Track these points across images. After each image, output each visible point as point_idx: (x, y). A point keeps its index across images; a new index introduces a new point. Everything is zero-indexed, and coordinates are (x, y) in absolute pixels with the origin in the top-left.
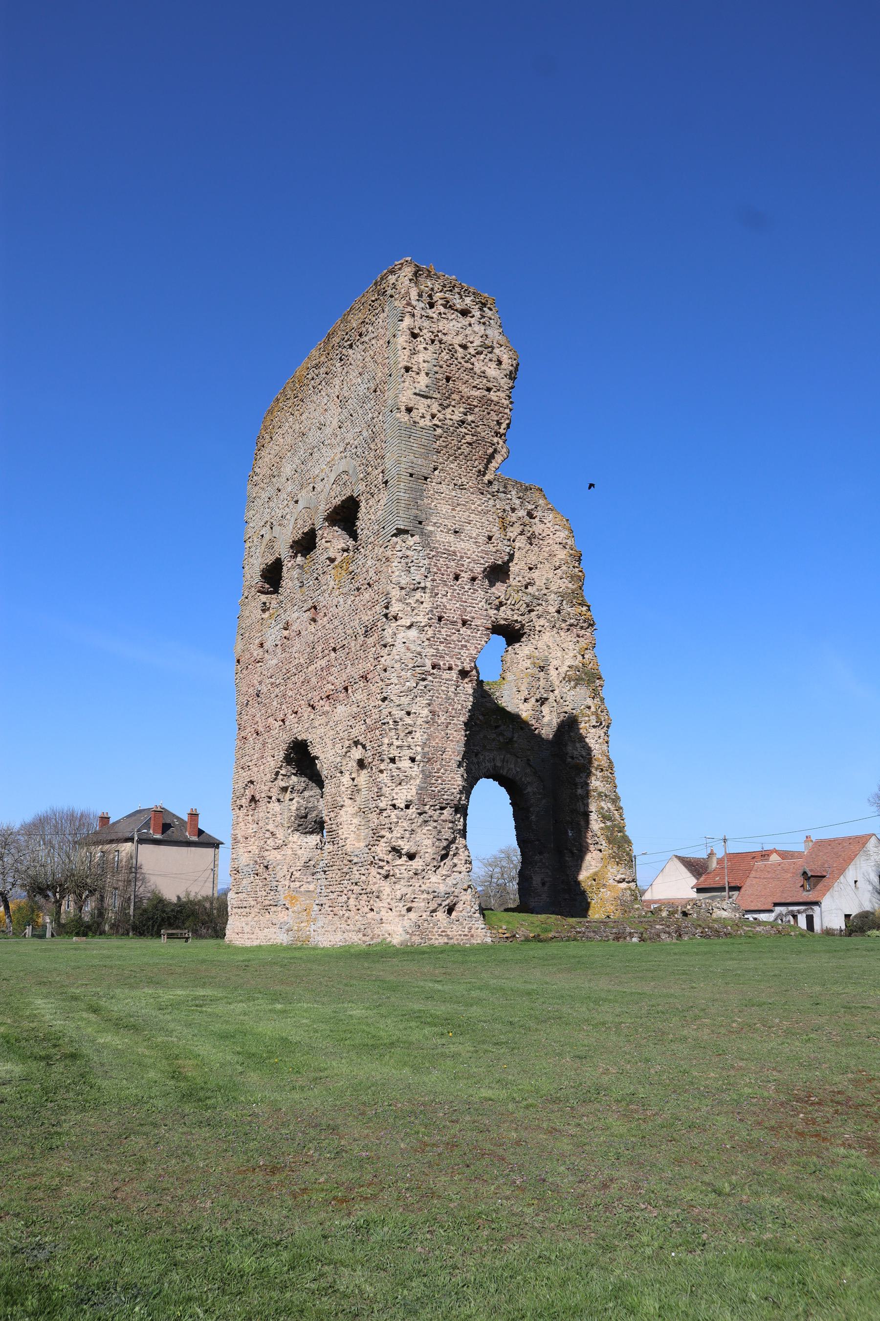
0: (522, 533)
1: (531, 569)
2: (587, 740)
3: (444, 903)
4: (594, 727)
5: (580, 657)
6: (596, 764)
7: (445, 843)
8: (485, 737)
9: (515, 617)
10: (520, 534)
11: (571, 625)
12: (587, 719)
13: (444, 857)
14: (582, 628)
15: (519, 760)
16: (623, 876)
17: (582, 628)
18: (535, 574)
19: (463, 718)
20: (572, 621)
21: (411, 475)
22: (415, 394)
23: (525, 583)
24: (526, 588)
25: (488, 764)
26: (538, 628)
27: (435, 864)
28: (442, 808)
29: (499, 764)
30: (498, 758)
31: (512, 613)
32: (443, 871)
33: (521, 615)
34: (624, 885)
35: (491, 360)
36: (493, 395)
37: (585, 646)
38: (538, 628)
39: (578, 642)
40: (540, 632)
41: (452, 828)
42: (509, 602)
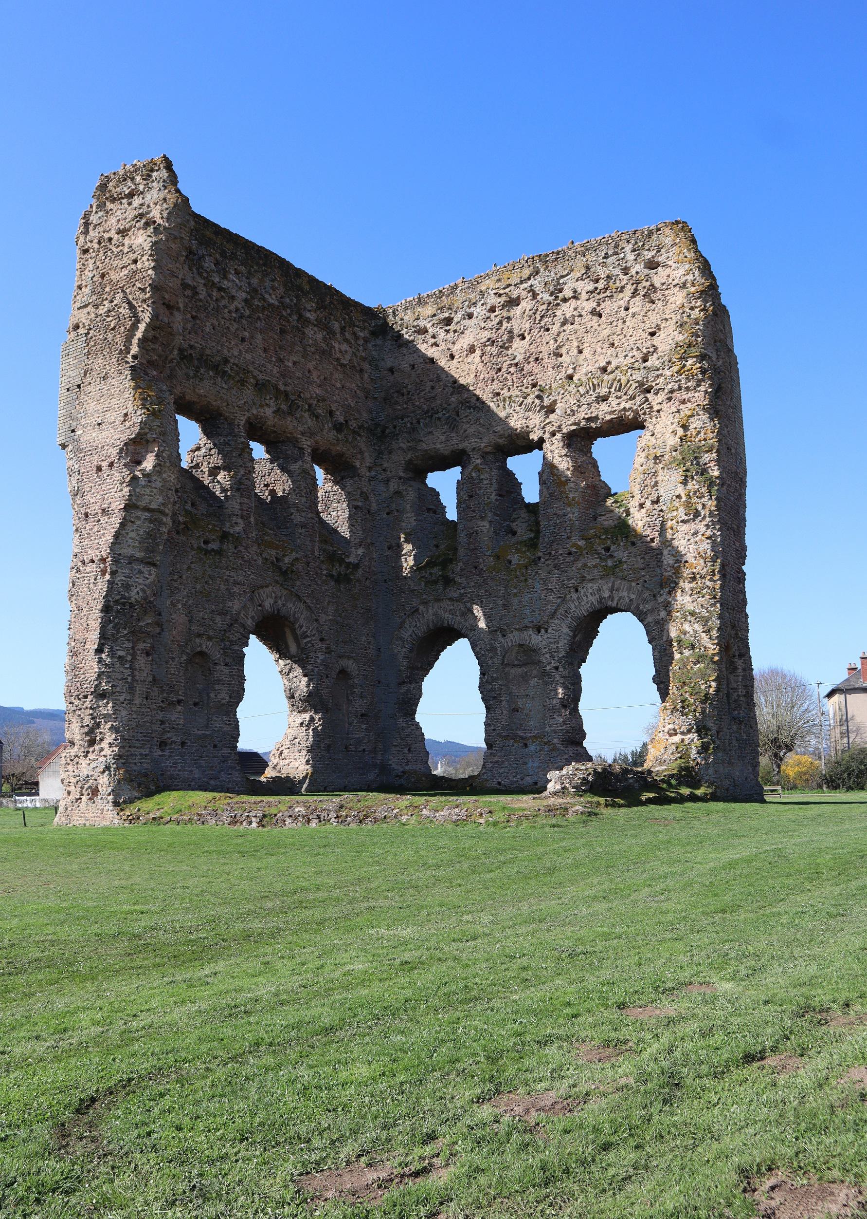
0: (635, 294)
1: (652, 334)
2: (675, 543)
3: (86, 786)
4: (683, 521)
5: (680, 432)
6: (686, 572)
7: (86, 729)
8: (585, 565)
9: (622, 407)
10: (632, 297)
11: (672, 391)
12: (675, 513)
13: (92, 742)
14: (688, 389)
15: (633, 584)
16: (671, 726)
17: (688, 389)
18: (656, 341)
19: (99, 607)
20: (670, 386)
21: (68, 390)
22: (79, 309)
23: (641, 355)
24: (645, 360)
25: (590, 598)
26: (656, 408)
27: (83, 750)
28: (86, 697)
29: (606, 595)
30: (605, 587)
31: (618, 401)
32: (91, 756)
33: (630, 399)
34: (677, 739)
35: (139, 229)
36: (139, 265)
37: (689, 413)
38: (656, 408)
39: (678, 411)
40: (658, 411)
41: (91, 715)
42: (613, 390)
